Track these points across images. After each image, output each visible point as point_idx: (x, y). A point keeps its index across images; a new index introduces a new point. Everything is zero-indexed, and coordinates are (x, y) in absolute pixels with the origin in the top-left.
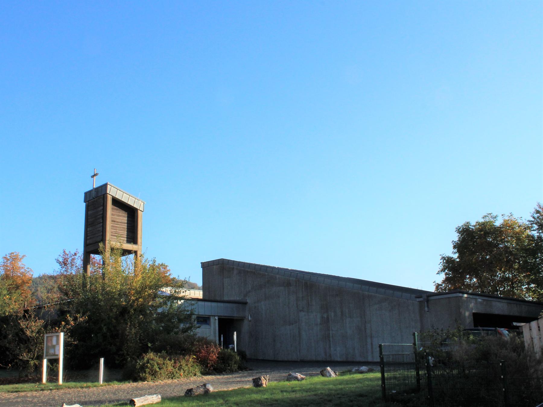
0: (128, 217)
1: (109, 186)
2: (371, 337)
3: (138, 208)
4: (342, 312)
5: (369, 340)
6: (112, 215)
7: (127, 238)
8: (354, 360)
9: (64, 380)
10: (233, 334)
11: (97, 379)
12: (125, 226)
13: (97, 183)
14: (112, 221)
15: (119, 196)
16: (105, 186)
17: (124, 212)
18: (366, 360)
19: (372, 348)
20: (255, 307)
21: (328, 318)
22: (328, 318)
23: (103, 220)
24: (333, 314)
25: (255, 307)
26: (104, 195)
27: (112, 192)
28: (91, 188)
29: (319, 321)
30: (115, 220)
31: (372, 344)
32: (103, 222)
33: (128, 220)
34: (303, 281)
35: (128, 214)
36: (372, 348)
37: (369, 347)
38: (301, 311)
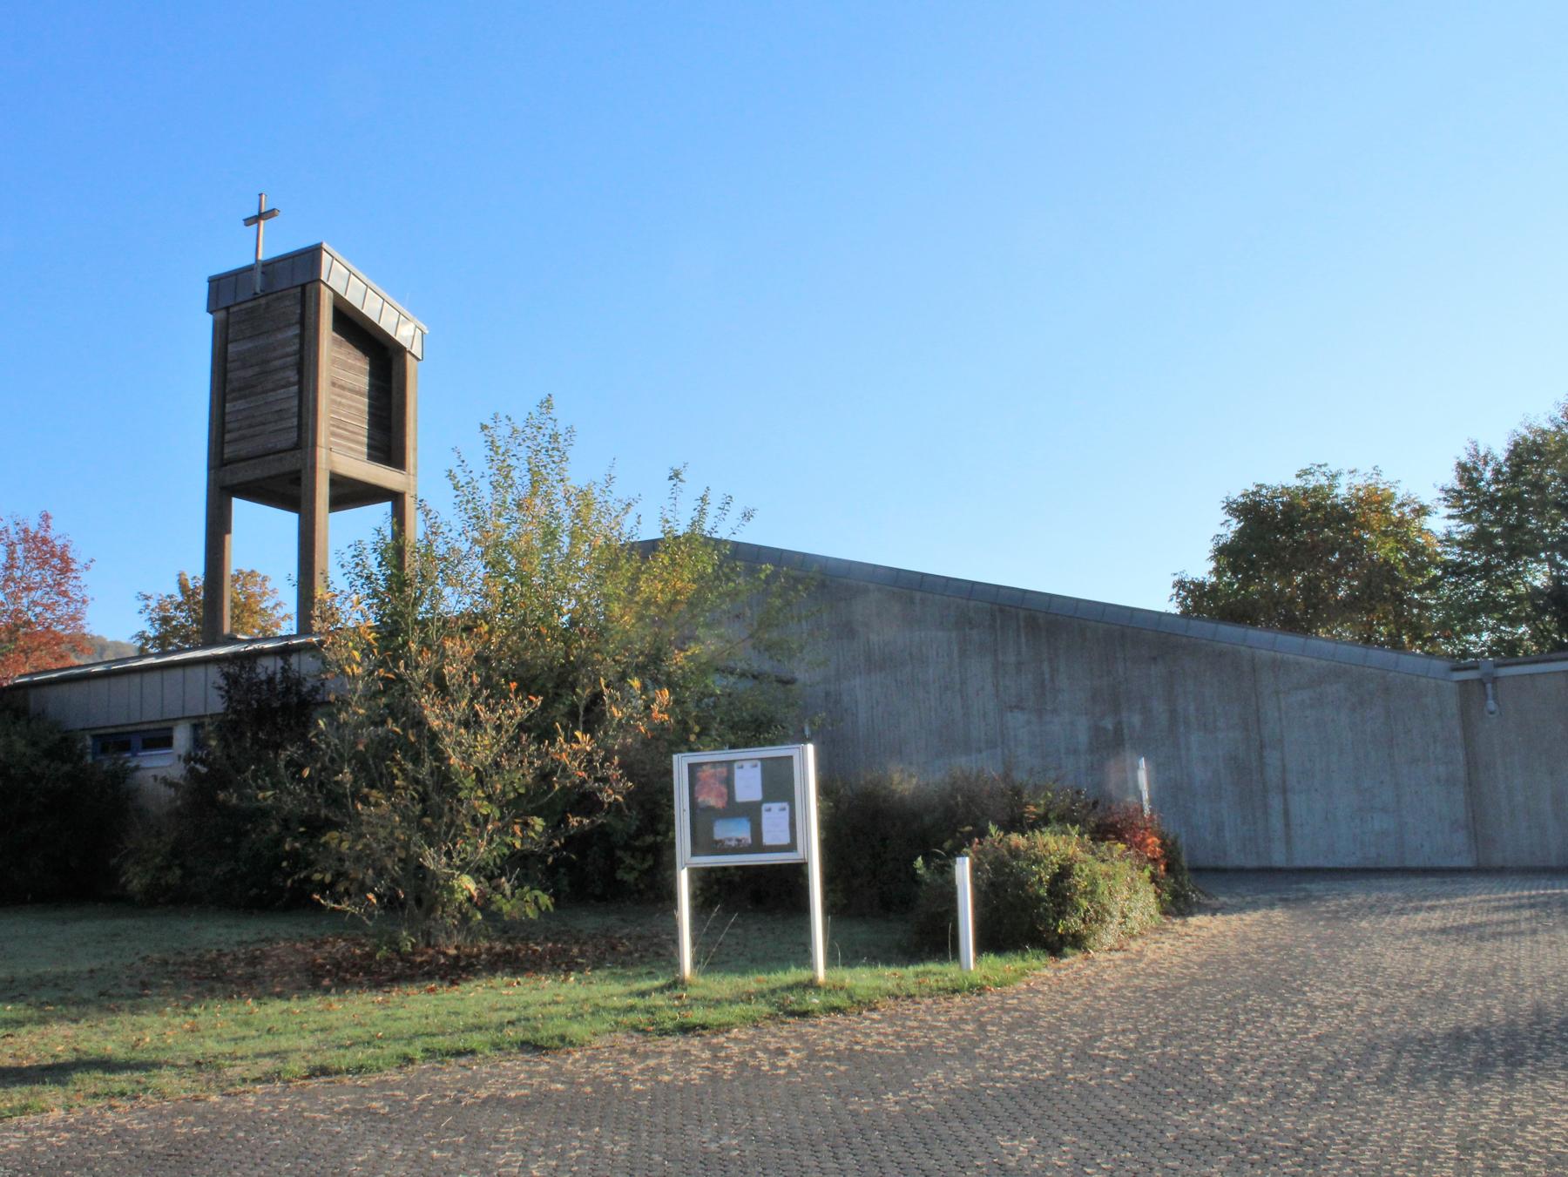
0: (372, 374)
1: (326, 258)
2: (1284, 790)
3: (408, 346)
4: (1173, 713)
5: (1276, 802)
6: (334, 361)
7: (370, 446)
8: (1221, 864)
9: (831, 960)
10: (1136, 768)
11: (661, 952)
12: (363, 403)
13: (274, 243)
14: (334, 384)
15: (354, 297)
16: (312, 255)
17: (359, 354)
18: (1264, 863)
19: (1287, 825)
20: (827, 694)
21: (1118, 730)
22: (1118, 730)
23: (300, 372)
24: (1136, 720)
25: (827, 694)
26: (303, 286)
27: (341, 278)
28: (250, 261)
29: (1083, 738)
30: (340, 375)
31: (1286, 813)
32: (300, 382)
33: (371, 385)
34: (1022, 614)
35: (372, 365)
36: (1287, 825)
37: (1277, 822)
38: (1011, 709)
